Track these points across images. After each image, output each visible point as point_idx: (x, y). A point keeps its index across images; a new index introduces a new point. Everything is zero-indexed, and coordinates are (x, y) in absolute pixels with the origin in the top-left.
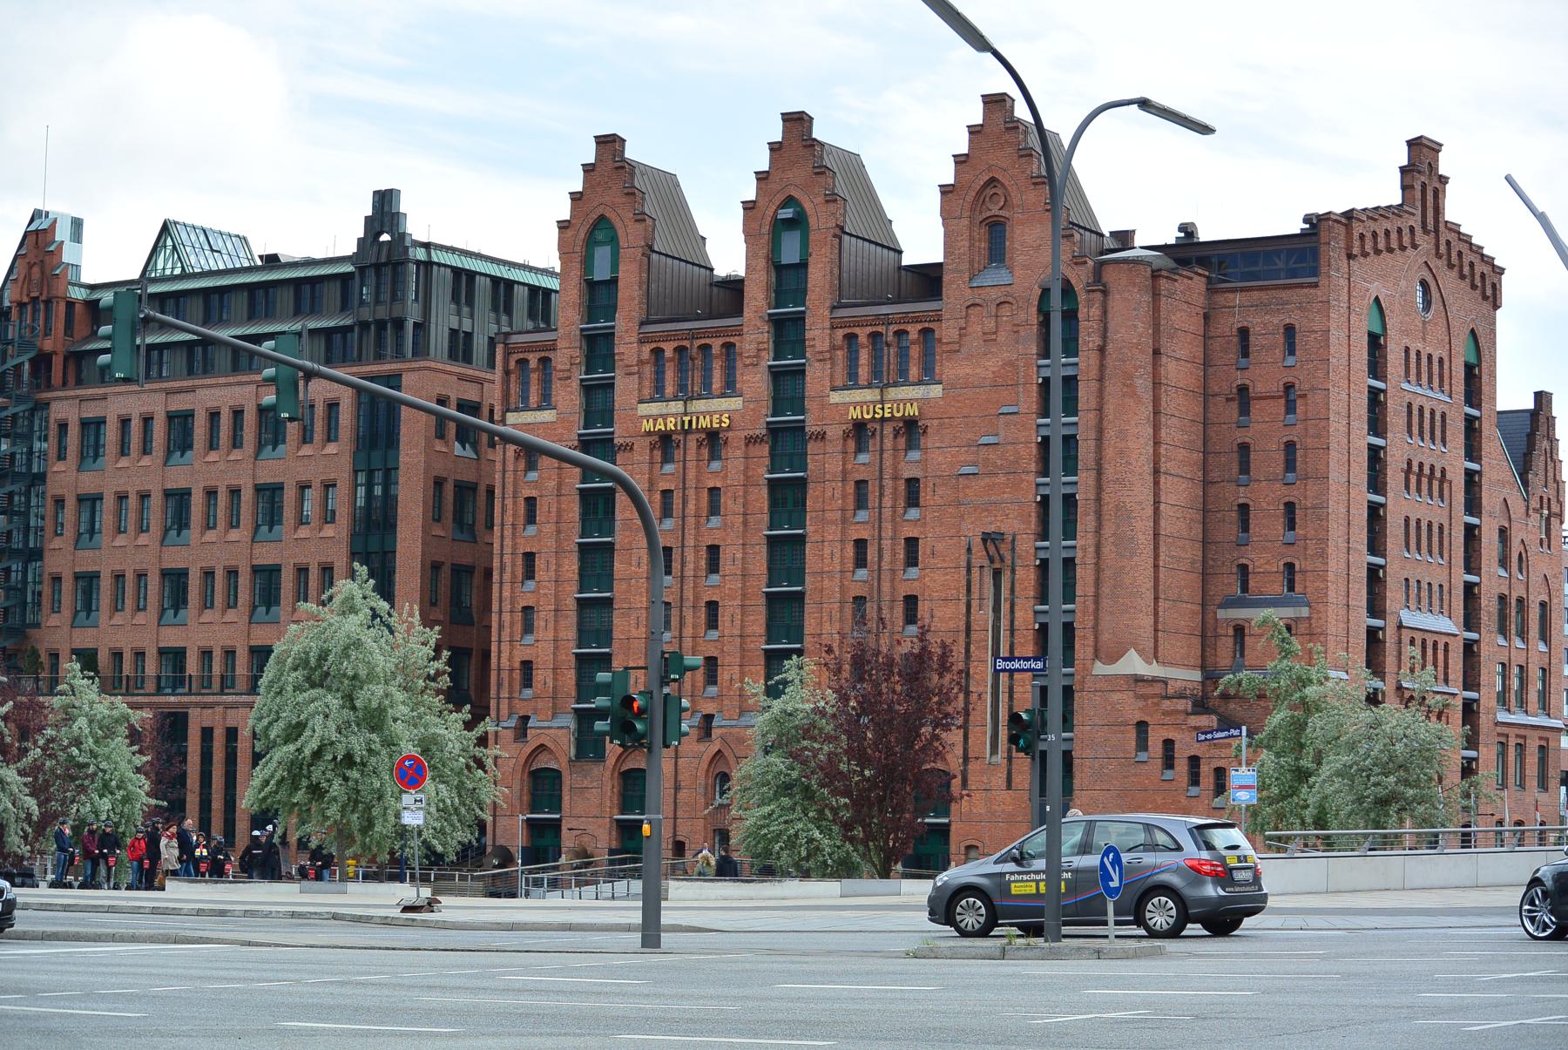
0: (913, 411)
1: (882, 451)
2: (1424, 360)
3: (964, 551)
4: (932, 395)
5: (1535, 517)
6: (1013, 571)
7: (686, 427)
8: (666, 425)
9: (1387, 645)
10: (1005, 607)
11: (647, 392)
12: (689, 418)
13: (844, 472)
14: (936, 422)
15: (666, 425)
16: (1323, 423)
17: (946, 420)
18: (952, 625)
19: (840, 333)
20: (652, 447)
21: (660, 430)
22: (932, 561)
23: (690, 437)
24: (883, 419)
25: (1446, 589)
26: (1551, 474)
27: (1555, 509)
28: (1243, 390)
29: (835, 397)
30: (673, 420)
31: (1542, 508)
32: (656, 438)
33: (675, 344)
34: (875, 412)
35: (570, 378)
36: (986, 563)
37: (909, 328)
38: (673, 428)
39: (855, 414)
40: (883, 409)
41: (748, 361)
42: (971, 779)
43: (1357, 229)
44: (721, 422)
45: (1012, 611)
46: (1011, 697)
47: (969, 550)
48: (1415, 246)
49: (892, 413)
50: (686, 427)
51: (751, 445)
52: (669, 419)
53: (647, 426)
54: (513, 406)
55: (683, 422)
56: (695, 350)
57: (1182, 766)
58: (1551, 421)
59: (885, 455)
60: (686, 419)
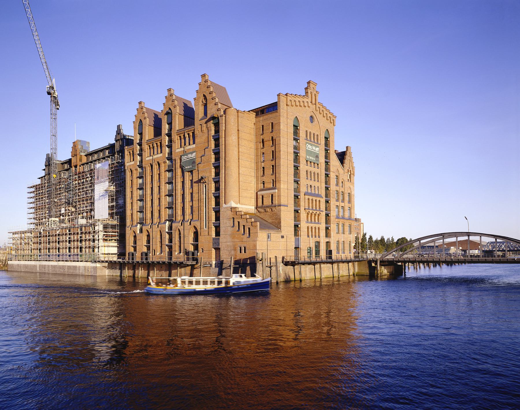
2: (312, 135)
5: (346, 174)
9: (301, 199)
16: (279, 145)
25: (320, 187)
26: (351, 165)
27: (352, 172)
28: (263, 140)
31: (348, 172)
42: (202, 233)
43: (289, 98)
46: (208, 214)
48: (309, 107)
57: (242, 228)
58: (350, 153)
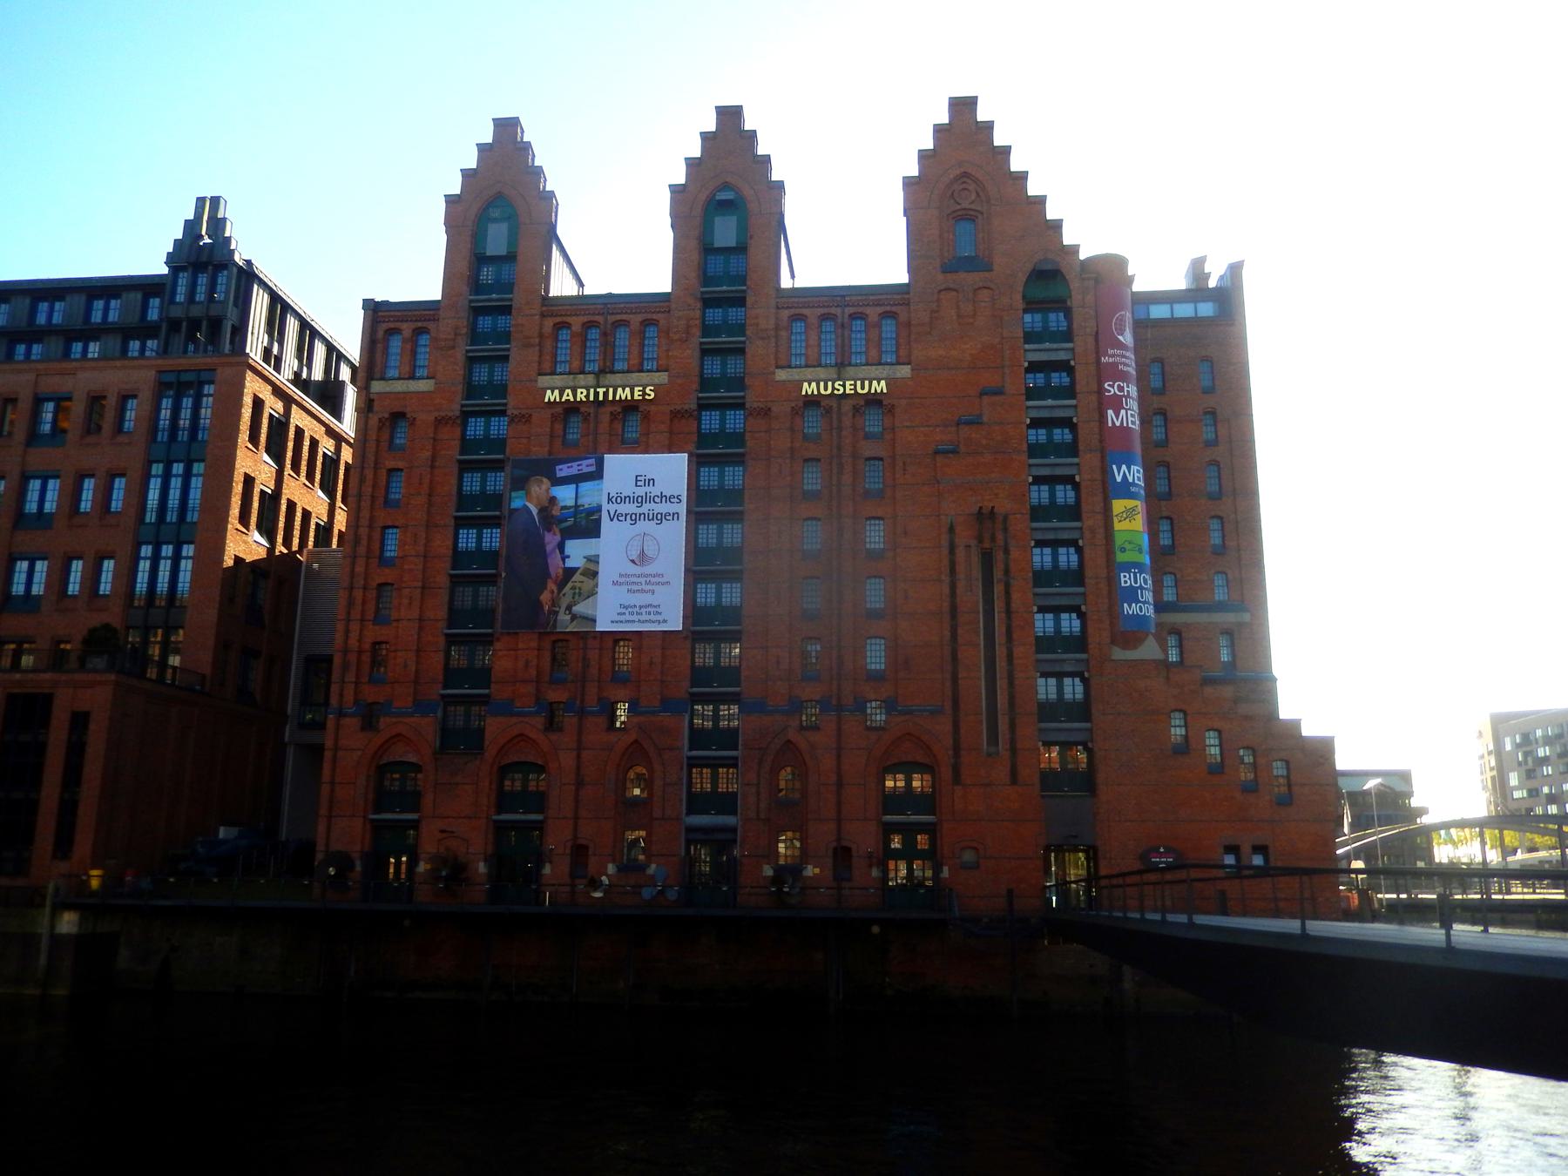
6: (1007, 551)
7: (601, 398)
8: (575, 396)
10: (998, 589)
11: (547, 366)
12: (605, 390)
13: (792, 449)
15: (575, 396)
20: (554, 418)
23: (602, 410)
30: (585, 392)
32: (559, 410)
35: (453, 347)
36: (973, 543)
38: (584, 399)
44: (644, 394)
45: (1007, 593)
47: (951, 529)
50: (601, 398)
52: (579, 391)
53: (550, 396)
54: (378, 375)
55: (597, 394)
60: (601, 391)
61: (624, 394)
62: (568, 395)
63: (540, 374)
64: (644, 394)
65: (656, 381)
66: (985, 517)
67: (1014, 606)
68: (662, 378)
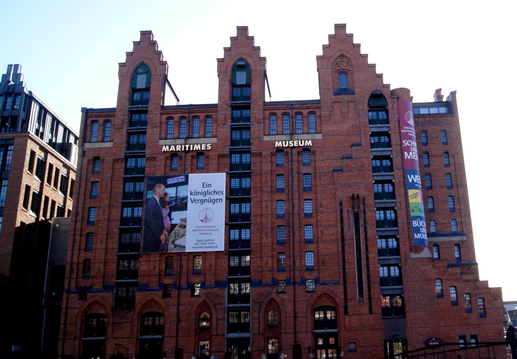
0: (309, 143)
1: (292, 161)
3: (338, 204)
4: (317, 138)
7: (187, 149)
10: (362, 229)
12: (189, 146)
14: (319, 149)
15: (176, 148)
17: (325, 149)
18: (334, 237)
19: (268, 112)
21: (172, 151)
22: (321, 209)
24: (294, 147)
29: (266, 138)
33: (180, 115)
34: (289, 144)
37: (303, 111)
39: (278, 144)
40: (293, 143)
41: (220, 123)
42: (350, 309)
44: (206, 147)
47: (341, 204)
49: (298, 144)
50: (187, 149)
51: (220, 159)
52: (177, 146)
55: (185, 148)
56: (191, 118)
59: (294, 163)
60: (187, 146)
61: (197, 147)
62: (173, 148)
63: (160, 139)
64: (206, 147)
65: (212, 142)
66: (355, 198)
67: (368, 236)
68: (214, 140)
